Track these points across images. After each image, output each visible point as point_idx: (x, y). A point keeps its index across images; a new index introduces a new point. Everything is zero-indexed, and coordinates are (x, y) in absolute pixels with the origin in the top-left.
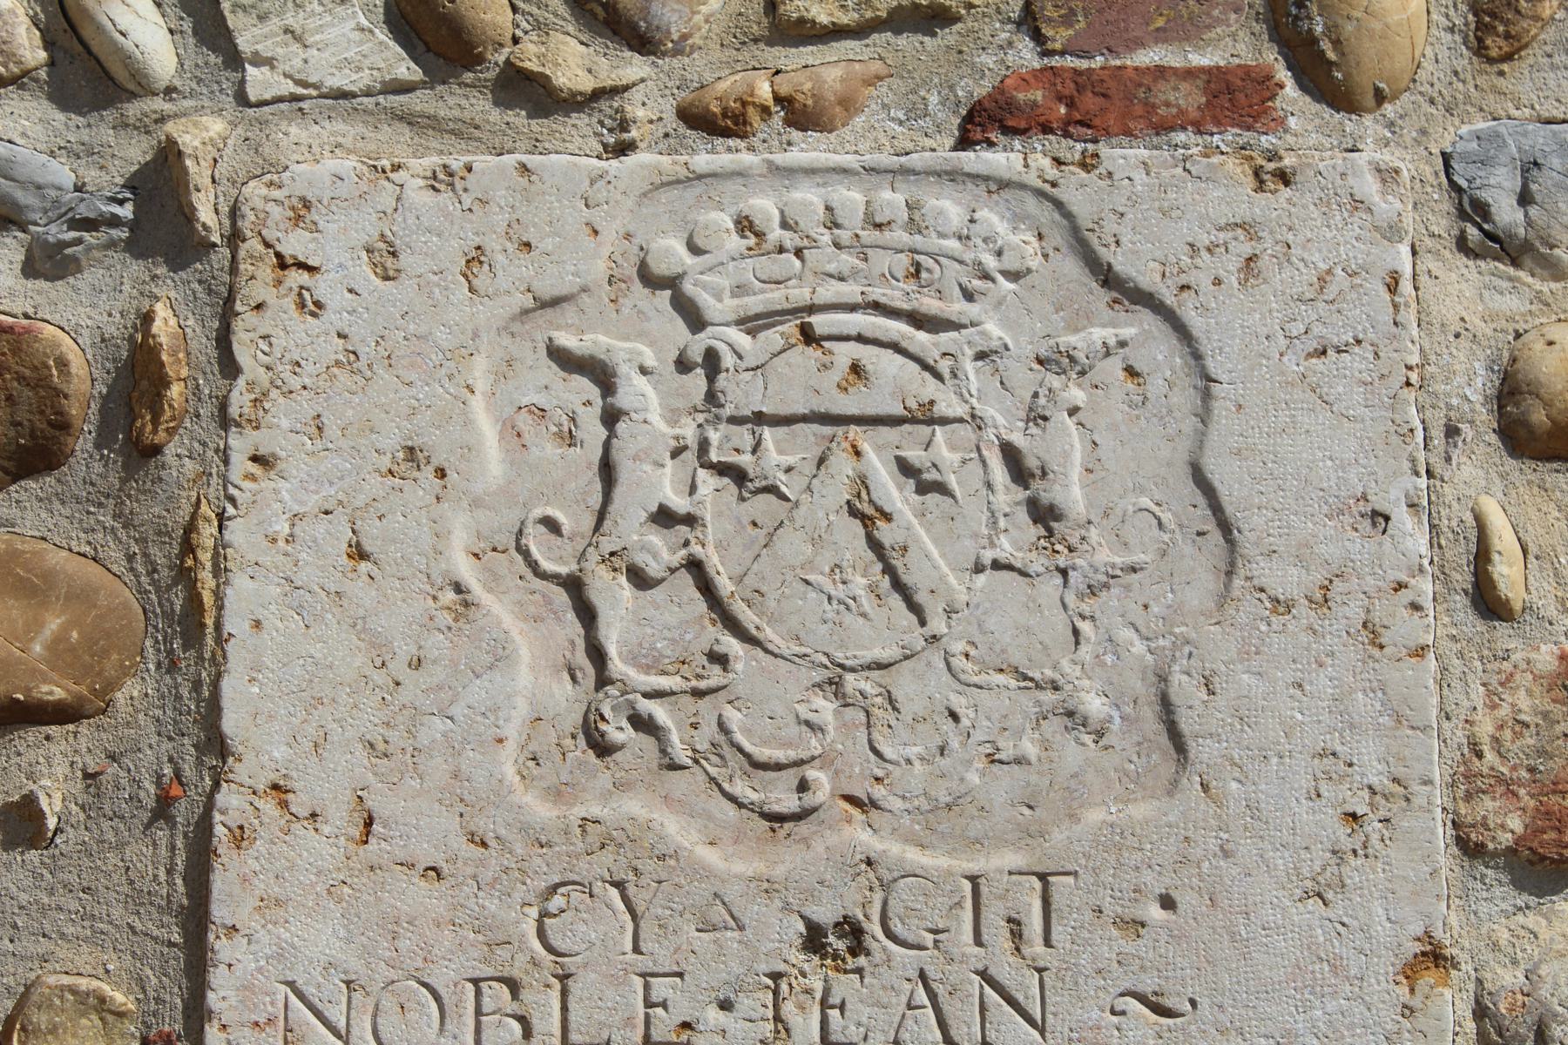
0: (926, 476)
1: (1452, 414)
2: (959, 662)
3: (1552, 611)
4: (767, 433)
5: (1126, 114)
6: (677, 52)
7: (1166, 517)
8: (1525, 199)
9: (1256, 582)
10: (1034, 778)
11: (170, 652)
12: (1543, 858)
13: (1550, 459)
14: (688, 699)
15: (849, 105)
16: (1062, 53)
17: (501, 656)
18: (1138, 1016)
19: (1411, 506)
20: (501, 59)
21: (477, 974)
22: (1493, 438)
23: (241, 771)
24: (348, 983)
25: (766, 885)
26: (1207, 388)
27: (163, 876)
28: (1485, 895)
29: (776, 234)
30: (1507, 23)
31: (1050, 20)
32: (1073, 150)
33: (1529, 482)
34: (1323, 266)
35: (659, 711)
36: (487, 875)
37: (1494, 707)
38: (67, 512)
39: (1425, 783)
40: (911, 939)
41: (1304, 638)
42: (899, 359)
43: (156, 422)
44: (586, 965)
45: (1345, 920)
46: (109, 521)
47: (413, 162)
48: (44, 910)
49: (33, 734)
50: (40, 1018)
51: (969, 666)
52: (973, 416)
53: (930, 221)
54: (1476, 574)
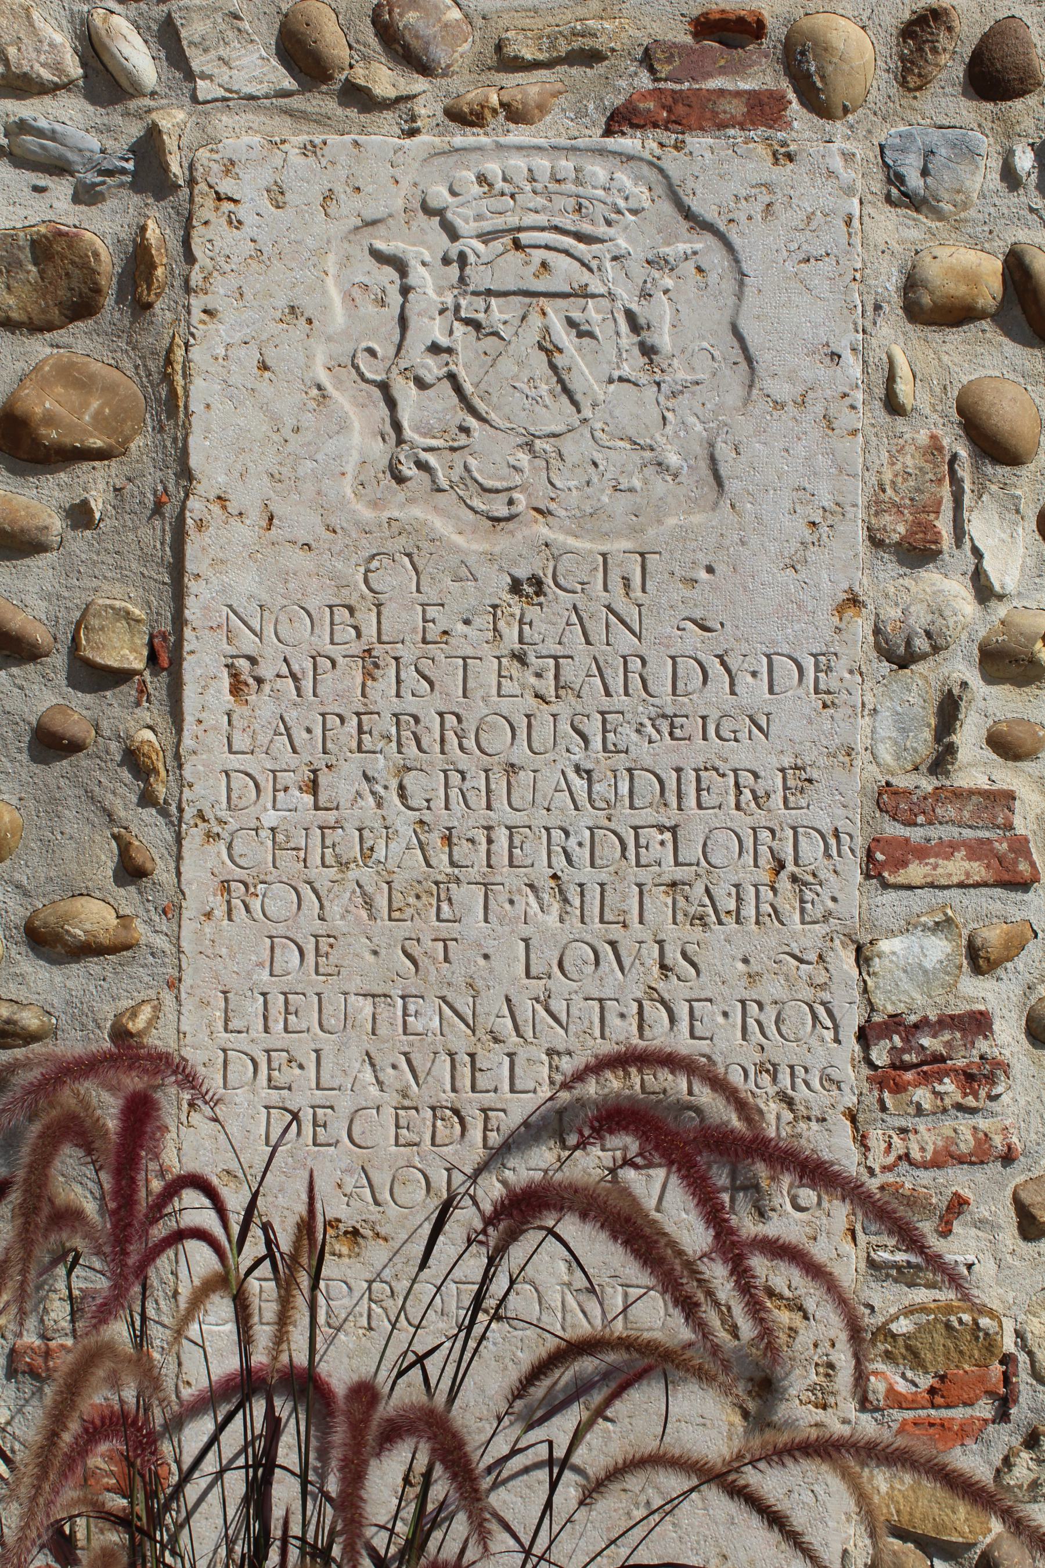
0: (582, 328)
2: (598, 434)
3: (927, 411)
4: (493, 301)
5: (701, 117)
6: (444, 75)
7: (716, 353)
8: (925, 173)
10: (638, 500)
11: (160, 421)
12: (915, 548)
13: (931, 324)
14: (448, 452)
15: (543, 109)
16: (666, 80)
17: (343, 427)
18: (692, 632)
19: (853, 350)
20: (343, 77)
21: (331, 603)
22: (900, 312)
23: (200, 488)
24: (261, 606)
27: (159, 546)
29: (500, 185)
30: (920, 67)
31: (659, 60)
32: (670, 138)
34: (810, 210)
35: (431, 459)
36: (336, 549)
37: (893, 464)
40: (569, 587)
41: (791, 424)
42: (569, 259)
43: (149, 289)
46: (124, 346)
47: (292, 139)
48: (94, 563)
49: (86, 466)
50: (95, 622)
51: (604, 436)
53: (587, 179)
54: (887, 389)
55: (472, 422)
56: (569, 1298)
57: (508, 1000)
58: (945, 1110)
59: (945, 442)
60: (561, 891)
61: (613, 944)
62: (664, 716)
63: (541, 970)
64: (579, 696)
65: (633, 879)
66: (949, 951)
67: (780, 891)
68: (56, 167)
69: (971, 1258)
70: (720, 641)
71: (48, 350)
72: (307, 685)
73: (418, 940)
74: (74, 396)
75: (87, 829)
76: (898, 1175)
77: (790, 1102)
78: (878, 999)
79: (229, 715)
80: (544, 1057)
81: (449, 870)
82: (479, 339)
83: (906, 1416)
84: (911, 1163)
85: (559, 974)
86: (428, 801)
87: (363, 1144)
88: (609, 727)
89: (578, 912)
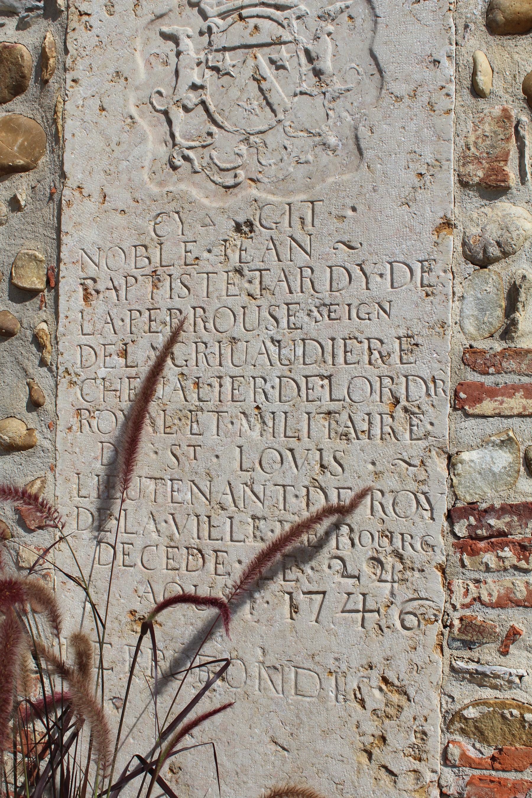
0: (278, 63)
1: (467, 20)
2: (288, 129)
4: (227, 54)
7: (360, 70)
9: (390, 91)
10: (311, 168)
11: (52, 146)
12: (490, 186)
13: (506, 35)
14: (201, 149)
17: (143, 139)
18: (342, 250)
19: (448, 57)
21: (136, 244)
22: (484, 28)
23: (69, 182)
24: (99, 248)
25: (222, 210)
26: (376, 20)
27: (52, 218)
28: (469, 201)
33: (498, 44)
35: (191, 154)
36: (138, 212)
37: (476, 130)
38: (27, 105)
39: (448, 161)
40: (268, 226)
41: (406, 110)
42: (271, 22)
44: (167, 240)
45: (416, 212)
46: (38, 107)
48: (22, 230)
49: (17, 176)
50: (19, 263)
51: (291, 130)
52: (295, 40)
54: (472, 81)
55: (214, 129)
56: (263, 671)
57: (230, 484)
58: (505, 570)
59: (513, 113)
60: (261, 417)
61: (291, 450)
62: (325, 305)
63: (249, 466)
64: (274, 294)
65: (304, 409)
66: (511, 460)
67: (396, 418)
68: (11, 12)
69: (521, 672)
70: (360, 255)
71: (4, 114)
72: (122, 293)
73: (180, 446)
74: (10, 137)
75: (16, 380)
76: (474, 611)
77: (401, 557)
78: (461, 492)
79: (82, 312)
80: (250, 520)
81: (197, 403)
82: (219, 78)
83: (475, 773)
84: (483, 604)
85: (259, 468)
86: (186, 361)
87: (149, 567)
88: (291, 313)
89: (271, 430)
